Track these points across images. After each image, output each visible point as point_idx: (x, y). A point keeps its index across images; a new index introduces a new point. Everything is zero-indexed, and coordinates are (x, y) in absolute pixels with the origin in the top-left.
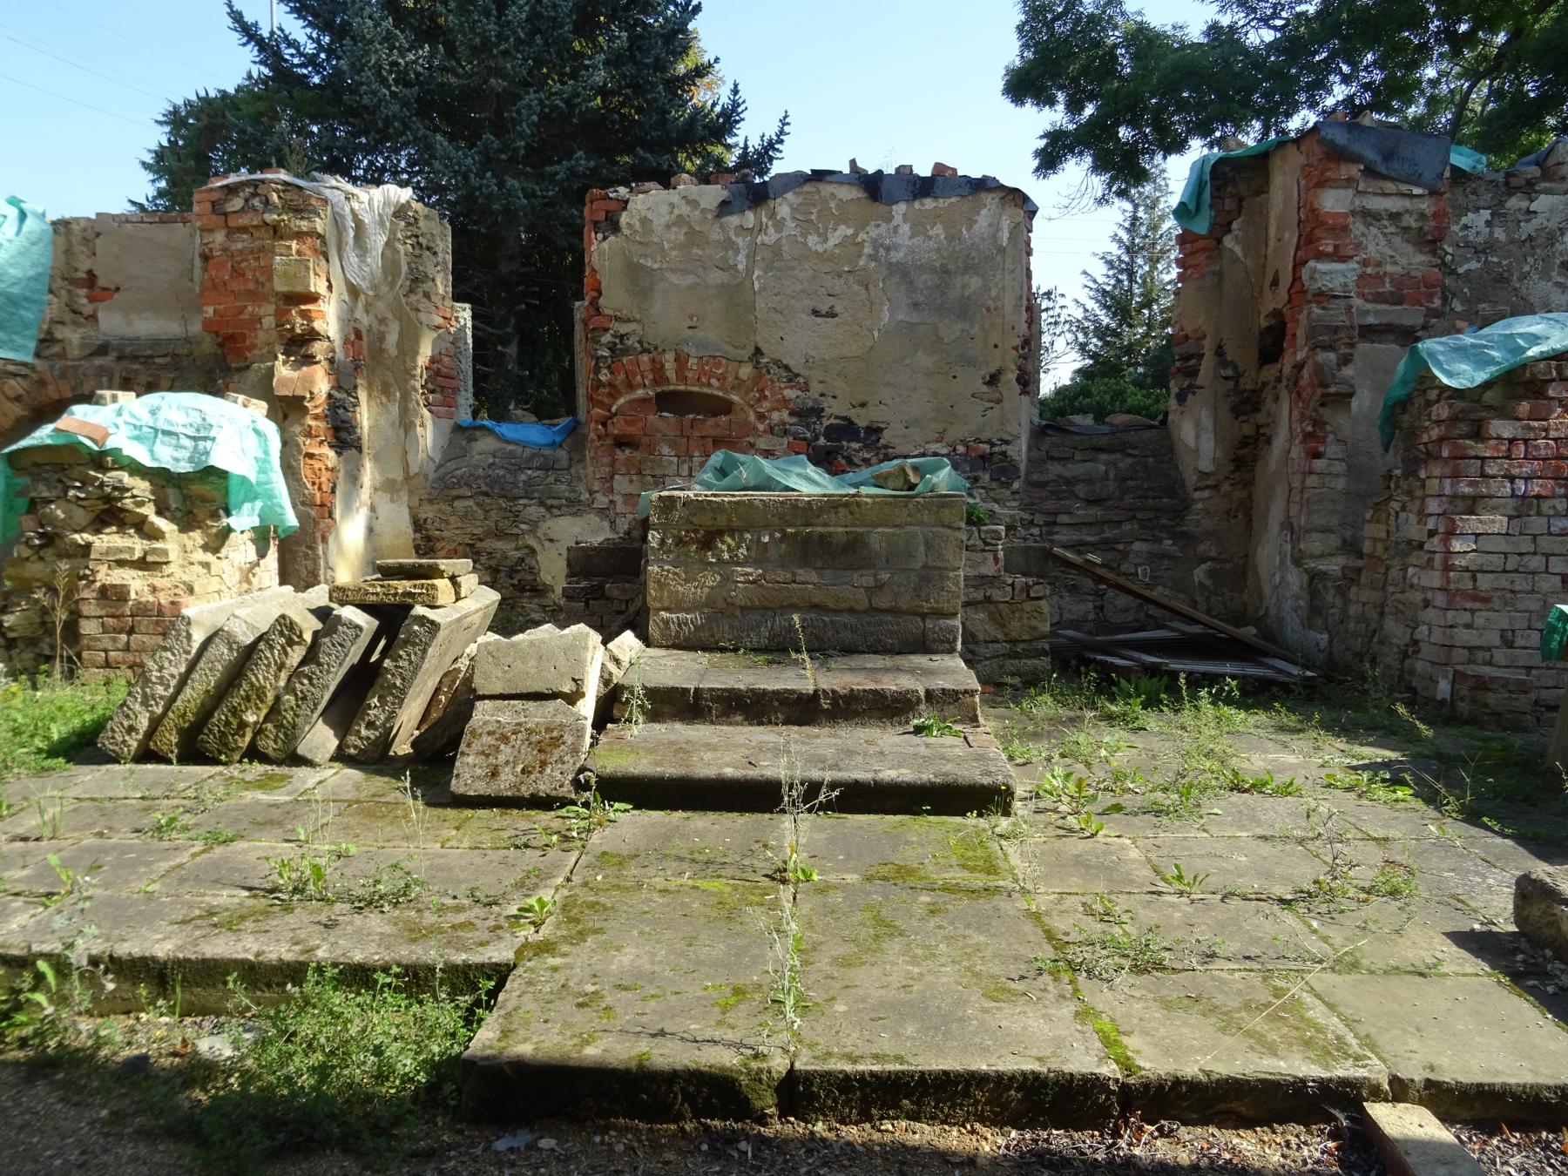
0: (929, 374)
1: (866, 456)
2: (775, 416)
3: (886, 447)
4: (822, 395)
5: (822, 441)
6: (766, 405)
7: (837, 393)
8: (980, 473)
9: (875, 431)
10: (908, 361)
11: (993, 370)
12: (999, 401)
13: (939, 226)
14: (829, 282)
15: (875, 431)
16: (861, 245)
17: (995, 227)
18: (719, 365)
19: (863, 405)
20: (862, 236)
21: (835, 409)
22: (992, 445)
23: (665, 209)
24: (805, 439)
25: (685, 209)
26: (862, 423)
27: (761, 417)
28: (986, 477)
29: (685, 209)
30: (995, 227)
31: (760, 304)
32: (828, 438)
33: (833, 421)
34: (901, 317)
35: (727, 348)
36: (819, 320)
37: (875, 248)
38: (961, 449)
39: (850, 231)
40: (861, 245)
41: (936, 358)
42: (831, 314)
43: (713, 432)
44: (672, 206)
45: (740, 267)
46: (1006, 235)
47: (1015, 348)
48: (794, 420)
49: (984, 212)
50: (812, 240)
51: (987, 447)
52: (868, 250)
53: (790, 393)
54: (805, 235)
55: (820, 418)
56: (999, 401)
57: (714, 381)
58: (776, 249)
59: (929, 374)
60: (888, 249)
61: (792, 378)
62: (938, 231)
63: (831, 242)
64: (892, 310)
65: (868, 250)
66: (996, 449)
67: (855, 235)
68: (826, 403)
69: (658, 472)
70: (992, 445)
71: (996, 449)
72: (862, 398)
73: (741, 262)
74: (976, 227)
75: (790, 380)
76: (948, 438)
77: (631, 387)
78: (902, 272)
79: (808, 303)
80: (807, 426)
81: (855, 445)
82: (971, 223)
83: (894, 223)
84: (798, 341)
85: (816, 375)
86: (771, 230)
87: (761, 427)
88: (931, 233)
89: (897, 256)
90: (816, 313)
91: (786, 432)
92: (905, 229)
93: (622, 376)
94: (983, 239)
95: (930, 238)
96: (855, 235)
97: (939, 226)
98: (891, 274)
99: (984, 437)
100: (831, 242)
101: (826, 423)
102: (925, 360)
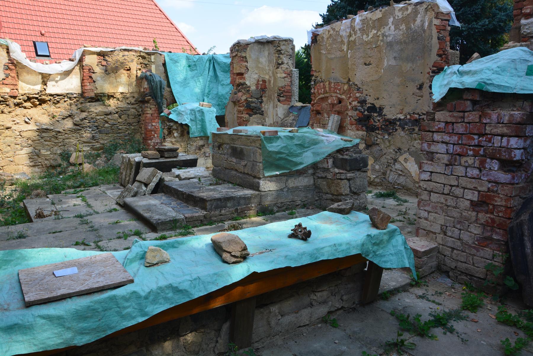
0: (398, 86)
1: (379, 119)
2: (353, 103)
3: (385, 115)
4: (367, 95)
5: (366, 113)
6: (351, 99)
7: (371, 94)
8: (415, 127)
9: (381, 109)
10: (392, 81)
11: (420, 82)
12: (422, 96)
13: (404, 25)
14: (369, 52)
15: (381, 109)
16: (378, 36)
17: (423, 22)
18: (339, 86)
19: (378, 99)
20: (379, 33)
21: (370, 100)
22: (420, 115)
23: (327, 33)
24: (361, 112)
25: (332, 32)
26: (377, 106)
27: (350, 104)
28: (417, 129)
29: (332, 32)
30: (423, 22)
31: (350, 63)
32: (368, 110)
33: (369, 105)
34: (390, 63)
35: (342, 79)
36: (366, 67)
37: (383, 37)
38: (408, 117)
39: (375, 32)
40: (378, 36)
41: (401, 79)
42: (369, 64)
43: (337, 109)
44: (329, 31)
45: (345, 50)
46: (426, 24)
47: (429, 73)
48: (359, 105)
49: (419, 16)
50: (365, 36)
51: (417, 116)
52: (381, 38)
53: (358, 95)
54: (362, 36)
55: (366, 104)
56: (422, 96)
57: (338, 91)
58: (354, 42)
59: (398, 86)
60: (387, 36)
61: (358, 89)
62: (403, 27)
63: (370, 36)
64: (388, 61)
65: (381, 38)
66: (421, 117)
67: (377, 33)
68: (368, 98)
69: (324, 123)
70: (420, 115)
71: (421, 117)
72: (377, 96)
73: (345, 48)
74: (416, 23)
75: (358, 90)
76: (404, 113)
77: (319, 94)
78: (390, 45)
79: (362, 61)
80: (362, 107)
81: (375, 115)
82: (415, 20)
83: (389, 26)
84: (361, 75)
85: (365, 87)
86: (353, 35)
87: (350, 107)
88: (401, 28)
89: (390, 39)
90: (365, 64)
91: (356, 110)
92: (393, 28)
93: (316, 91)
94: (419, 27)
95: (400, 30)
96: (377, 33)
97: (404, 25)
98: (388, 46)
99: (416, 112)
100: (370, 37)
101: (368, 106)
102: (397, 80)
